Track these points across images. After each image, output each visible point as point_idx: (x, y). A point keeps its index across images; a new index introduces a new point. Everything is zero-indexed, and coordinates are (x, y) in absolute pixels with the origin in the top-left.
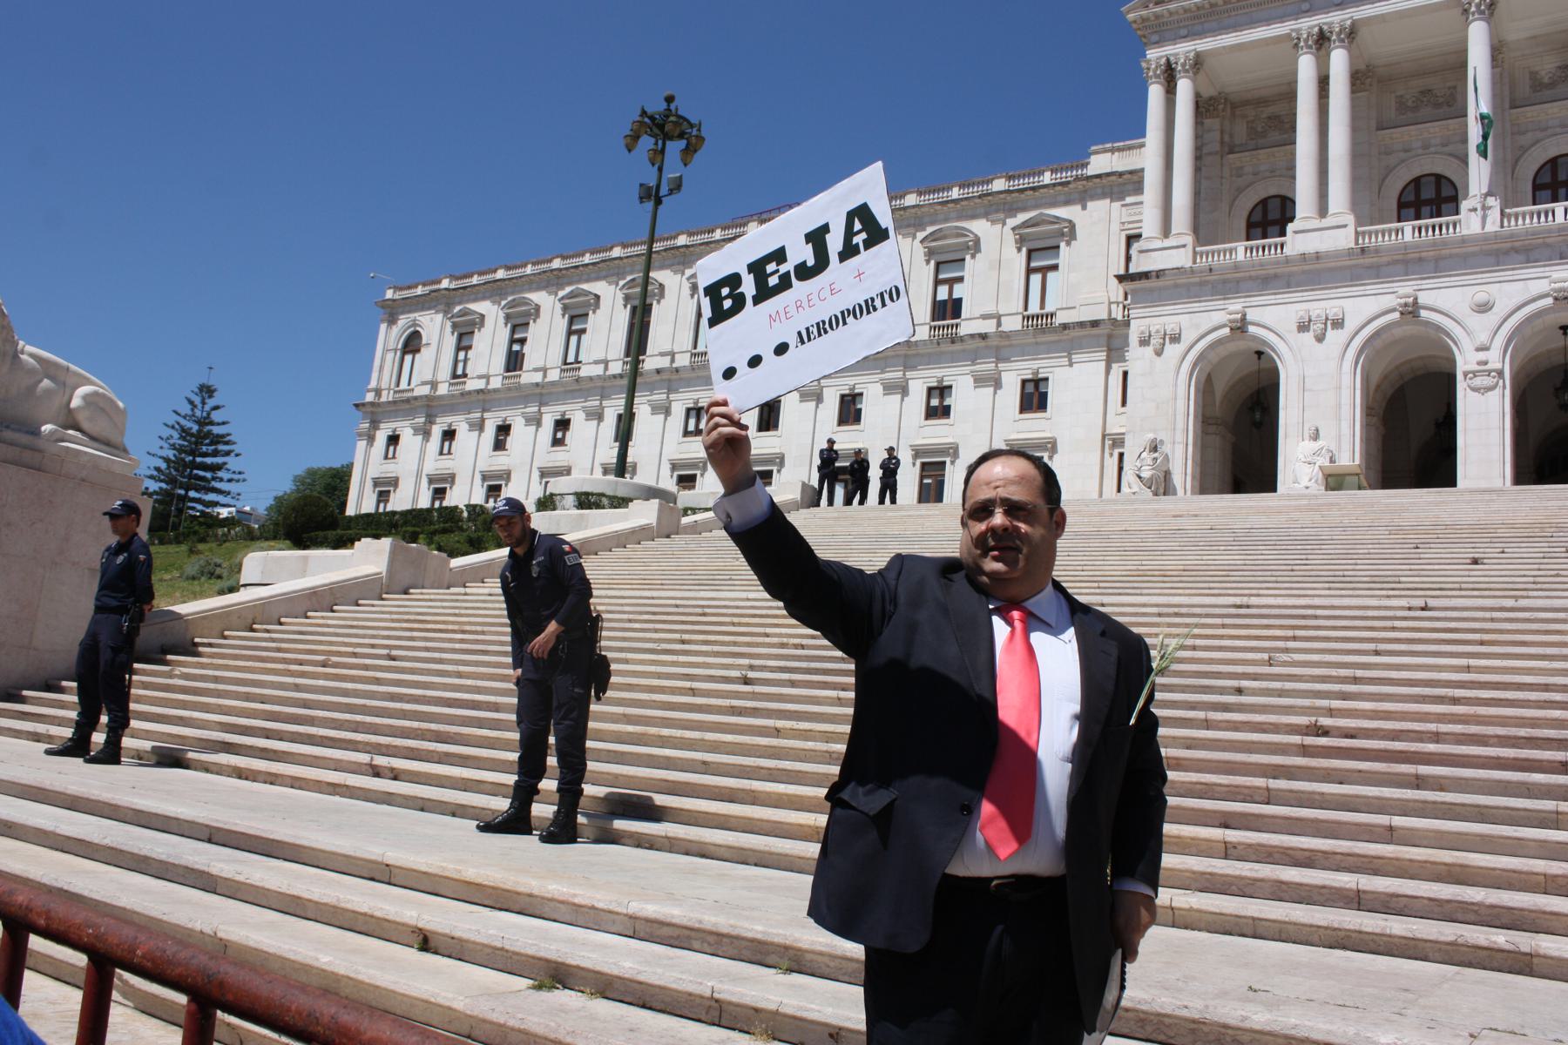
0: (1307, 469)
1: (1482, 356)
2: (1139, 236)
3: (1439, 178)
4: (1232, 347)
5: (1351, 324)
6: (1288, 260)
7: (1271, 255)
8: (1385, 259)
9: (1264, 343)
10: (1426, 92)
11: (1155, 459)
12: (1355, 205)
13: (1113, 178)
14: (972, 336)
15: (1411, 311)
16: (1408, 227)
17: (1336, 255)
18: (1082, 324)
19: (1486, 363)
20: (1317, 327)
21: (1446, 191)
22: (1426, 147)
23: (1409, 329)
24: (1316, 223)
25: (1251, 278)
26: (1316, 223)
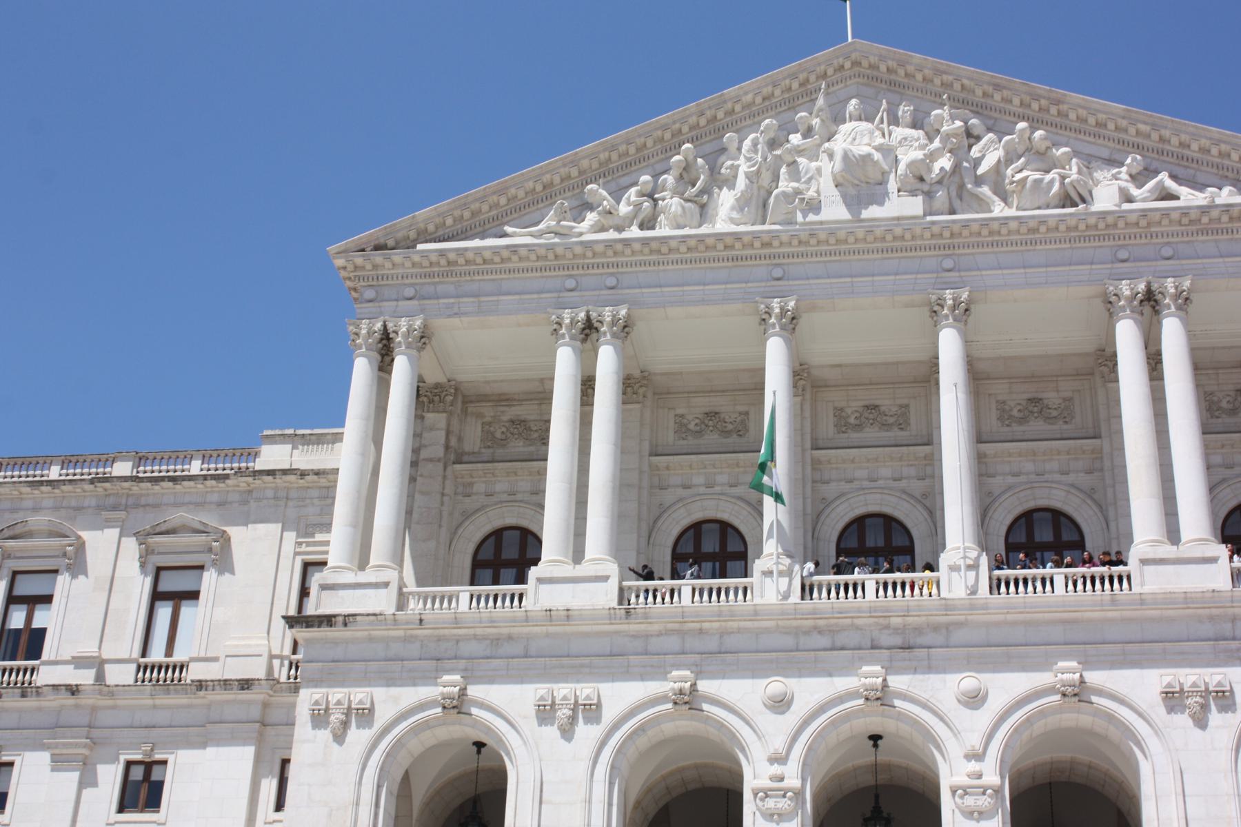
1: (776, 769)
2: (324, 563)
3: (725, 528)
5: (610, 714)
7: (504, 610)
8: (656, 628)
9: (489, 730)
10: (712, 414)
12: (617, 551)
13: (292, 478)
14: (55, 687)
15: (688, 700)
16: (686, 586)
17: (592, 616)
18: (226, 684)
19: (782, 779)
20: (563, 713)
21: (733, 547)
22: (709, 486)
23: (685, 725)
24: (569, 570)
25: (475, 637)
26: (569, 570)
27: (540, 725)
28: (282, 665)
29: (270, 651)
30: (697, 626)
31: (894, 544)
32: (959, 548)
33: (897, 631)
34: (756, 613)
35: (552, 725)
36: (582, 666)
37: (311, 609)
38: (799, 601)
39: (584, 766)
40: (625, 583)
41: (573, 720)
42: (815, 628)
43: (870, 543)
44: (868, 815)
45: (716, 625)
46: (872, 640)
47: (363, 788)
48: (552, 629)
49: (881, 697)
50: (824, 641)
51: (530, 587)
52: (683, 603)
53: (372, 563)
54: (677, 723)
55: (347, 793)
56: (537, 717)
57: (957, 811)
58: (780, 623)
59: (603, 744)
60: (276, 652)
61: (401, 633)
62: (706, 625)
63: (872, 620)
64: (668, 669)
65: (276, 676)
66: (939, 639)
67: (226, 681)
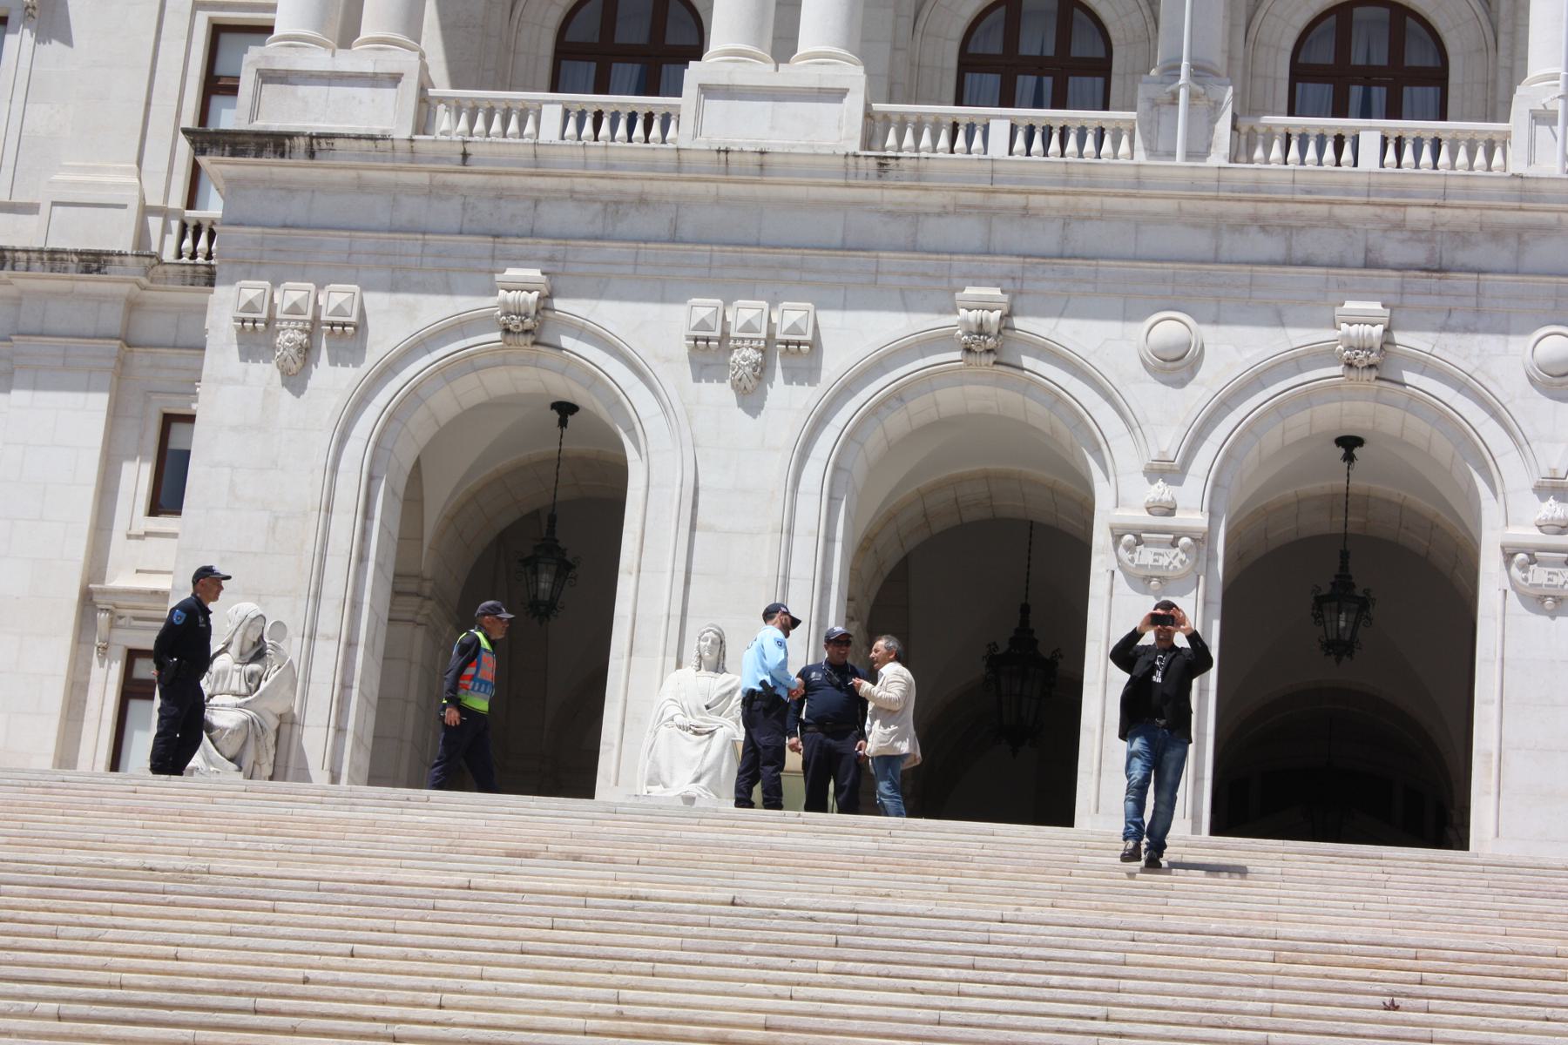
0: (692, 748)
1: (1160, 491)
2: (268, 30)
4: (500, 382)
5: (836, 362)
6: (680, 164)
7: (616, 144)
8: (935, 199)
9: (594, 380)
11: (254, 680)
12: (862, 43)
15: (992, 346)
16: (1000, 121)
17: (811, 167)
18: (53, 258)
19: (1170, 511)
20: (744, 356)
21: (1083, 46)
23: (981, 394)
24: (763, 73)
25: (572, 194)
26: (763, 73)
27: (697, 379)
28: (166, 229)
29: (143, 199)
30: (1020, 200)
31: (1407, 64)
32: (1555, 77)
33: (1417, 234)
34: (1139, 182)
35: (722, 380)
36: (786, 266)
37: (229, 117)
38: (1225, 163)
39: (778, 465)
40: (877, 107)
41: (762, 371)
42: (1255, 218)
43: (1358, 59)
44: (1326, 590)
45: (1055, 201)
46: (1367, 250)
47: (340, 479)
48: (727, 189)
49: (1376, 364)
50: (1271, 246)
51: (687, 100)
52: (991, 154)
53: (365, 33)
54: (971, 389)
55: (310, 489)
56: (692, 361)
57: (1512, 594)
58: (1186, 205)
59: (820, 422)
60: (154, 200)
61: (423, 178)
62: (1036, 201)
63: (1370, 210)
64: (956, 282)
65: (155, 248)
66: (1503, 256)
67: (53, 252)
